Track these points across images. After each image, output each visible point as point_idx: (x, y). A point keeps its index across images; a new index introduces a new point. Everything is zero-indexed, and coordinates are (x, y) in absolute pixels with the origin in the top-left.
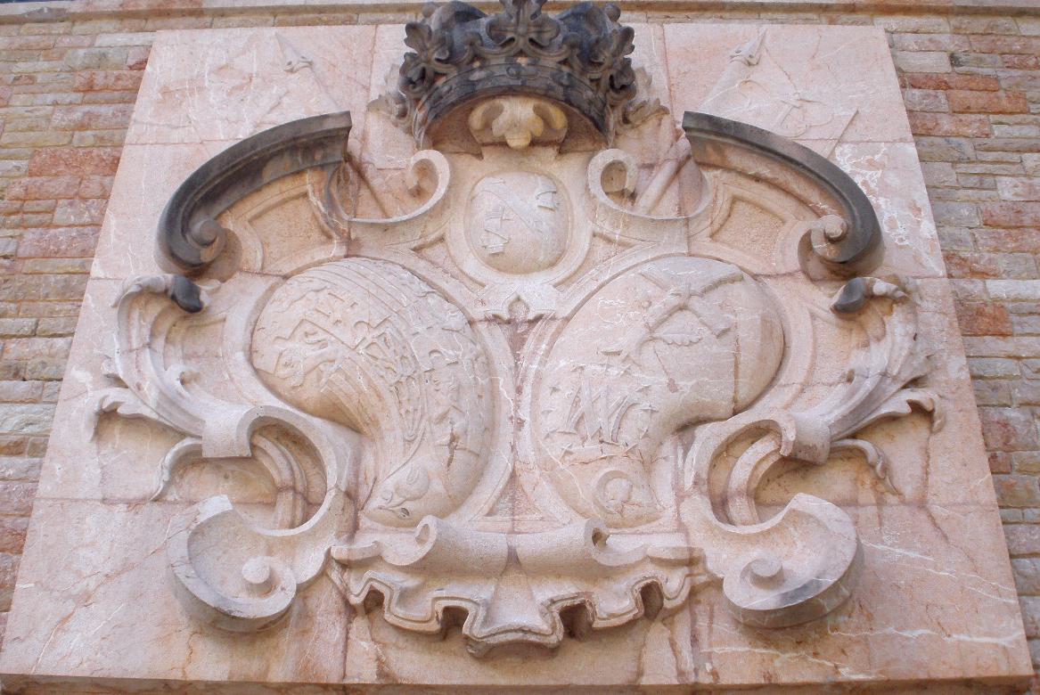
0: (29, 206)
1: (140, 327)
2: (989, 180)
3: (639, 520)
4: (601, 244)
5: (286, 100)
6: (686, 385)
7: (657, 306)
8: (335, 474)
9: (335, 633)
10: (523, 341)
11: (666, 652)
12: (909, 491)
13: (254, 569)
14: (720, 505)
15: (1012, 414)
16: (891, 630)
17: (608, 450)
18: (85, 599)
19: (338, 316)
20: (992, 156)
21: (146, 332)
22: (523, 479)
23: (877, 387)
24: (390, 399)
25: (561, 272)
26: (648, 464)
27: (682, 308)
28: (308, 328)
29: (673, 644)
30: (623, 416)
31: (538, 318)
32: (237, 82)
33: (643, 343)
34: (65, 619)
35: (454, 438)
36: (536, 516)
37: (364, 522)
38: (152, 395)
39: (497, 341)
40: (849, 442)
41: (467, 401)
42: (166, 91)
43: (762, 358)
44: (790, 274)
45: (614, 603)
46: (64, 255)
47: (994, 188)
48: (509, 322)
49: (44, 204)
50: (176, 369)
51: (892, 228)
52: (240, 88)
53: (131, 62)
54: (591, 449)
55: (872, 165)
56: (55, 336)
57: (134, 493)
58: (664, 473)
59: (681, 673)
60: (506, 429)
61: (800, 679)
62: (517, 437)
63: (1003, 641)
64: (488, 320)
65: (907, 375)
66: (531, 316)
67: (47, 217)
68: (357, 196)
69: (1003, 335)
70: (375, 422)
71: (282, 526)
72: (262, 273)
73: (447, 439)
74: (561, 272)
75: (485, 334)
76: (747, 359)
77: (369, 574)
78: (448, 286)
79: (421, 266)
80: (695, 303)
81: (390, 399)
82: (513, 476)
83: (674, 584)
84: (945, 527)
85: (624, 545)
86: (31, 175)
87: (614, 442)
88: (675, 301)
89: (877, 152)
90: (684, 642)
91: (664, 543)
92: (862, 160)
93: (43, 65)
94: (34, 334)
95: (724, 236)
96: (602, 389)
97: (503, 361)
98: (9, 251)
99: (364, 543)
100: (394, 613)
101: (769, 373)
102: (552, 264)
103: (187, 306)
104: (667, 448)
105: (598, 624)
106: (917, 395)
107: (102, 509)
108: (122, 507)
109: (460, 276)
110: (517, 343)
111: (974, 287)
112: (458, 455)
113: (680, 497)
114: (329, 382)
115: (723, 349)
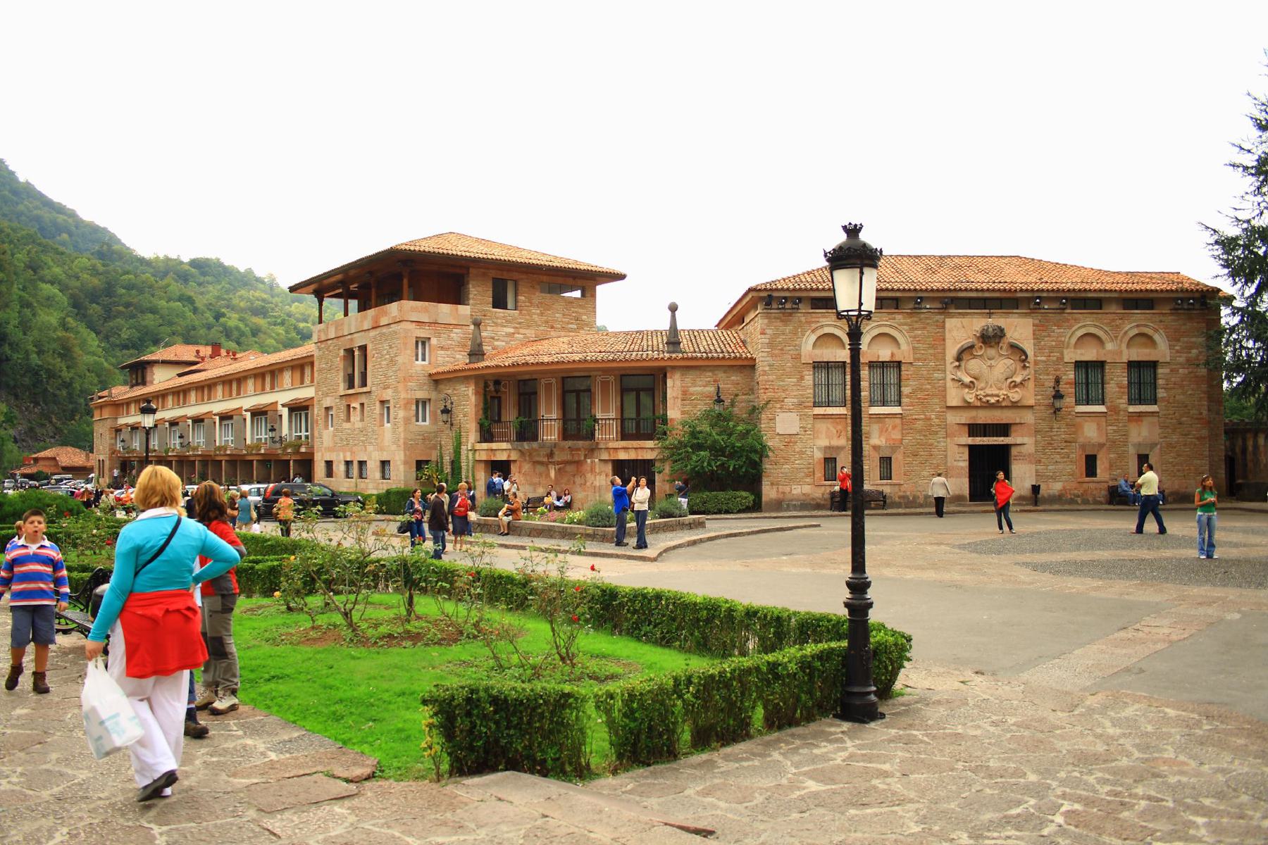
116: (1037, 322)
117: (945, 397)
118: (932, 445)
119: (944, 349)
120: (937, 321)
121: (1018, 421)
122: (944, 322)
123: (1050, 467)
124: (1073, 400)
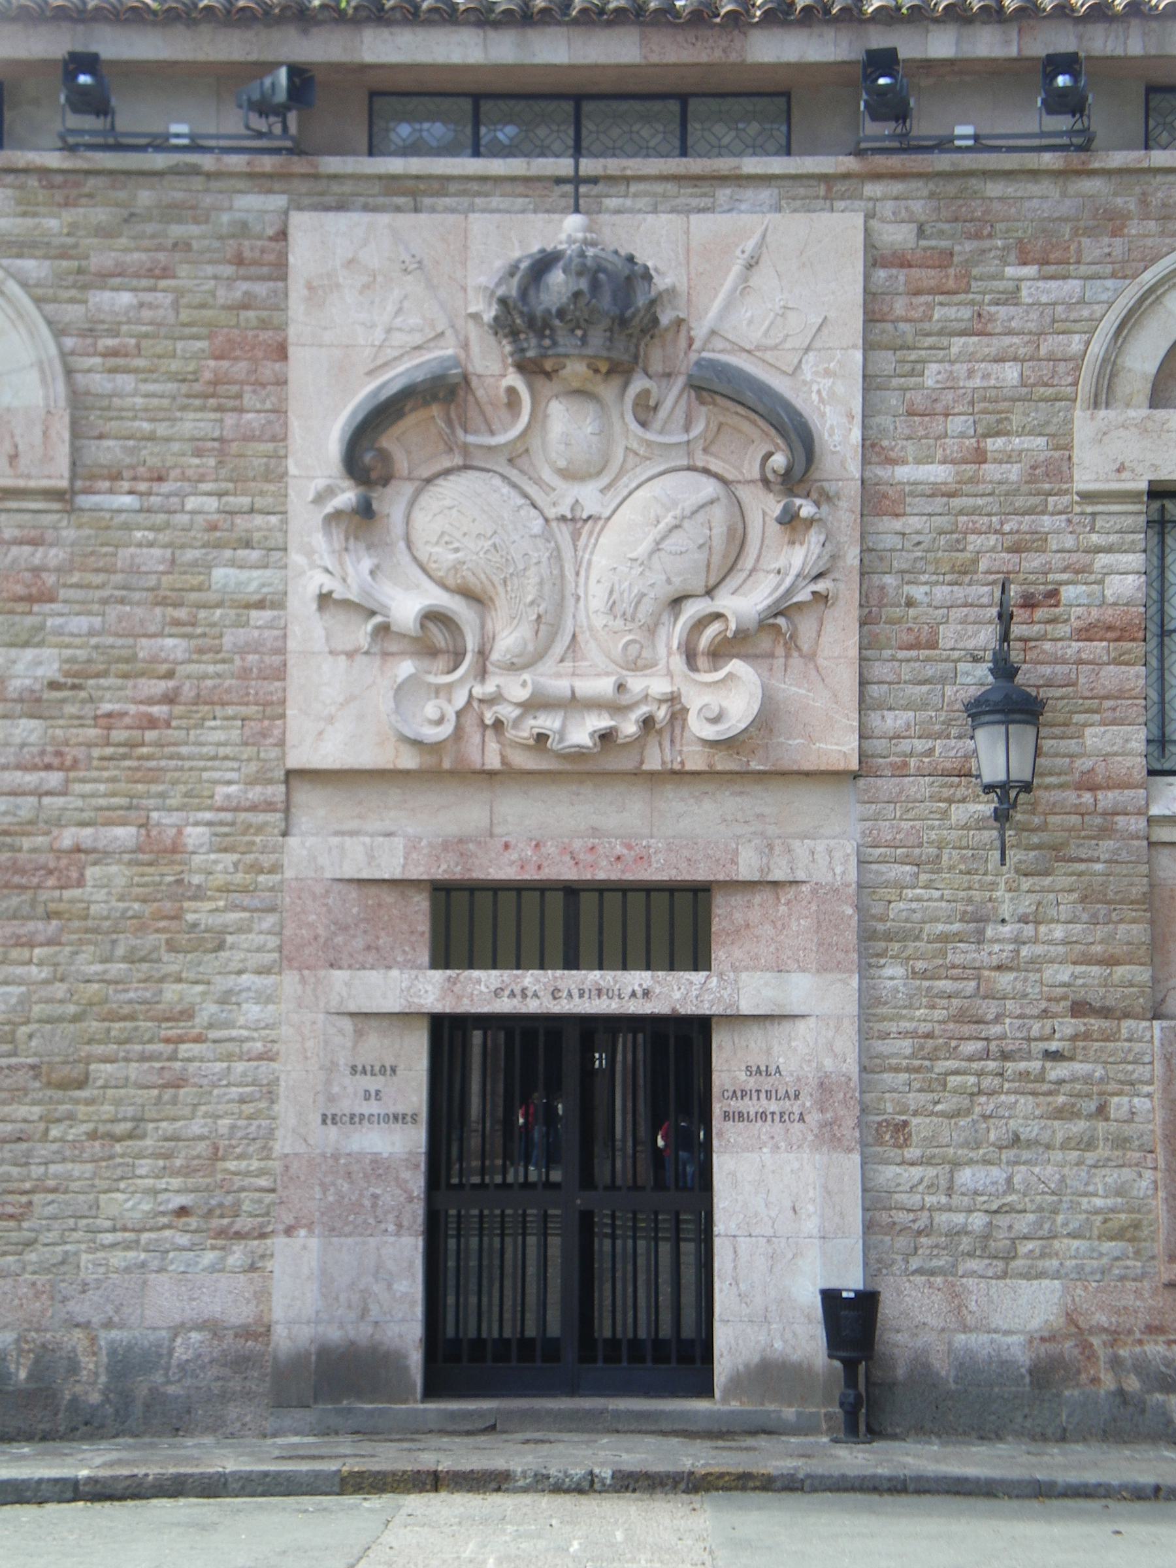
0: (221, 389)
1: (338, 535)
2: (919, 366)
3: (646, 667)
4: (631, 455)
5: (406, 304)
6: (677, 581)
7: (662, 526)
8: (471, 643)
9: (477, 739)
10: (580, 534)
11: (657, 749)
12: (805, 648)
13: (431, 710)
14: (690, 657)
15: (890, 580)
16: (782, 739)
17: (630, 626)
18: (331, 719)
19: (465, 529)
20: (930, 341)
21: (342, 537)
22: (580, 638)
23: (793, 584)
24: (501, 589)
25: (604, 481)
26: (652, 630)
27: (677, 527)
28: (447, 538)
29: (660, 745)
30: (638, 603)
31: (590, 517)
32: (365, 279)
33: (651, 554)
34: (321, 733)
35: (539, 617)
36: (587, 663)
37: (490, 668)
38: (355, 587)
39: (563, 534)
40: (771, 621)
41: (547, 588)
42: (310, 287)
43: (725, 556)
44: (753, 481)
45: (629, 727)
46: (259, 439)
47: (922, 375)
48: (573, 520)
49: (235, 389)
50: (367, 563)
51: (831, 435)
52: (366, 287)
53: (270, 232)
54: (619, 623)
55: (827, 373)
56: (269, 513)
57: (349, 647)
58: (662, 632)
59: (663, 763)
60: (571, 601)
61: (727, 768)
62: (576, 608)
63: (844, 749)
64: (558, 519)
65: (814, 573)
66: (585, 516)
67: (237, 403)
68: (465, 401)
69: (897, 515)
70: (491, 599)
71: (443, 673)
72: (409, 479)
73: (534, 617)
74: (604, 481)
75: (556, 530)
76: (716, 559)
77: (495, 708)
78: (532, 490)
79: (514, 474)
80: (686, 524)
81: (501, 589)
82: (574, 636)
83: (662, 713)
84: (823, 672)
85: (636, 684)
86: (217, 358)
87: (633, 620)
88: (674, 522)
89: (832, 360)
90: (667, 744)
91: (659, 686)
92: (821, 368)
93: (194, 230)
94: (252, 511)
95: (713, 449)
96: (627, 584)
97: (568, 553)
98: (217, 434)
99: (489, 688)
100: (510, 733)
101: (730, 564)
102: (599, 473)
103: (365, 512)
104: (665, 617)
105: (620, 741)
106: (821, 586)
107: (330, 658)
108: (343, 657)
109: (538, 482)
110: (576, 536)
111: (883, 472)
112: (542, 627)
113: (669, 654)
114: (463, 577)
115: (702, 556)
116: (897, 236)
117: (274, 710)
118: (188, 1014)
119: (280, 411)
120: (242, 230)
121: (746, 869)
122: (282, 235)
123: (965, 1176)
124: (1137, 738)
